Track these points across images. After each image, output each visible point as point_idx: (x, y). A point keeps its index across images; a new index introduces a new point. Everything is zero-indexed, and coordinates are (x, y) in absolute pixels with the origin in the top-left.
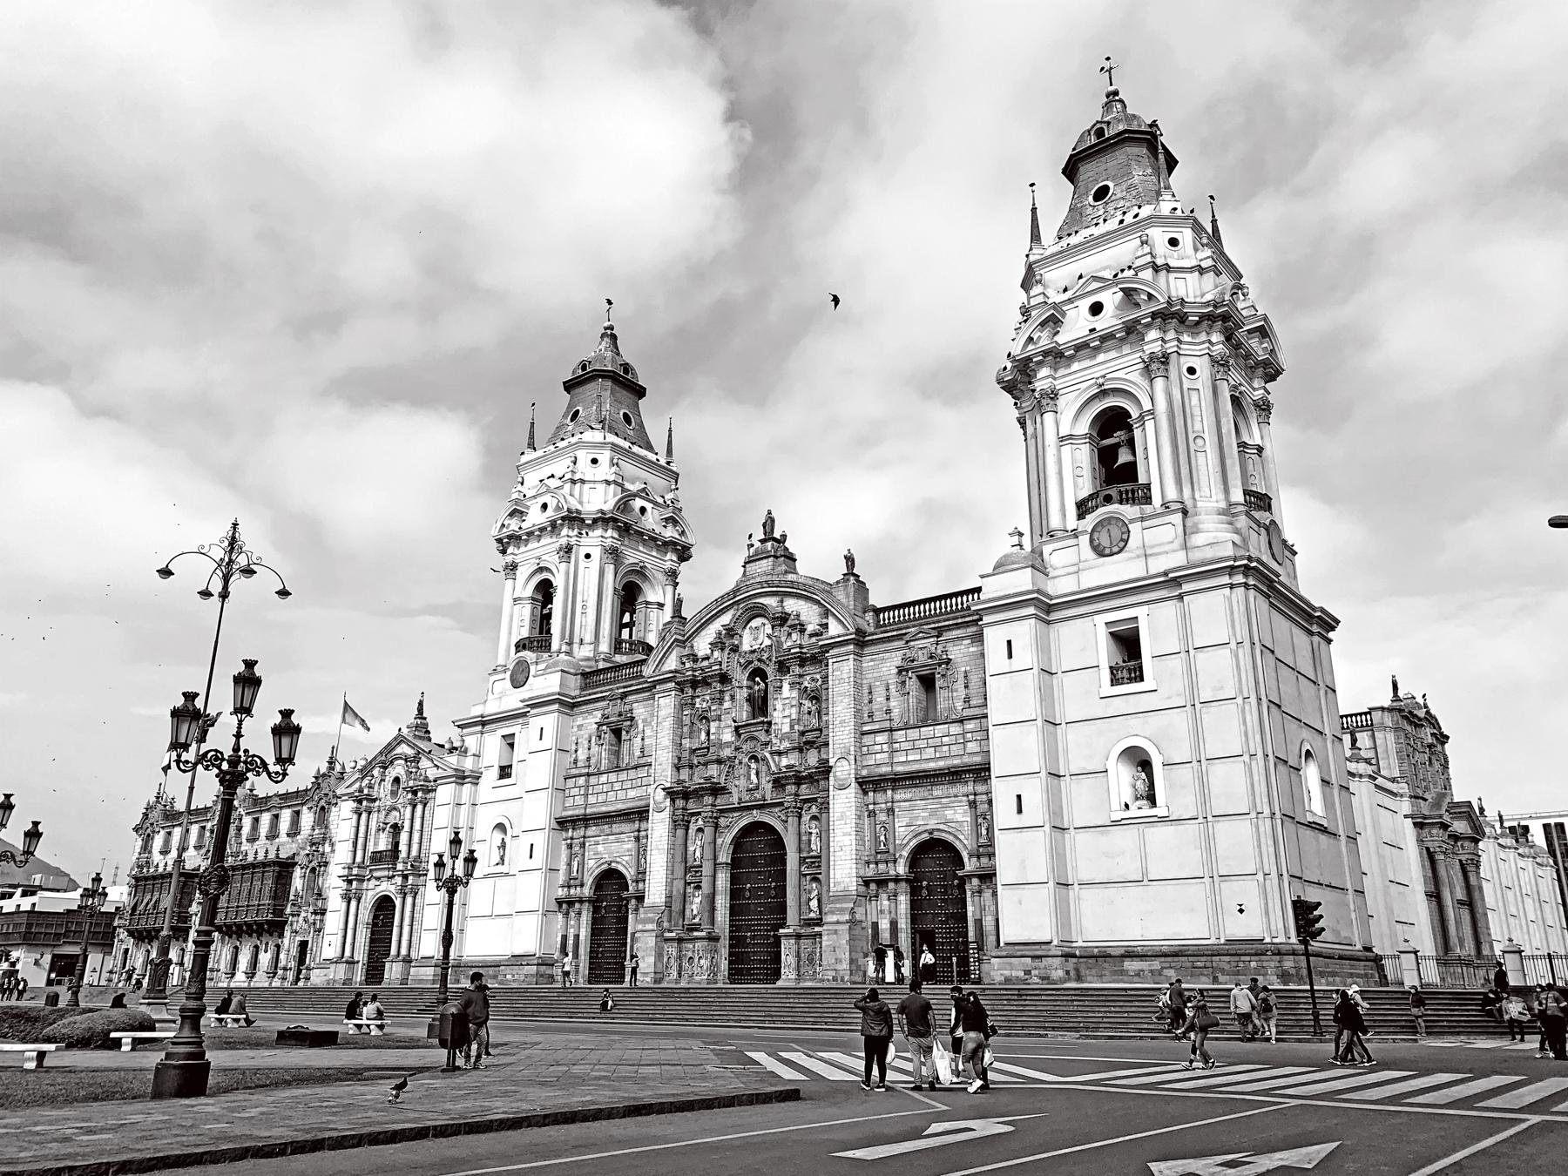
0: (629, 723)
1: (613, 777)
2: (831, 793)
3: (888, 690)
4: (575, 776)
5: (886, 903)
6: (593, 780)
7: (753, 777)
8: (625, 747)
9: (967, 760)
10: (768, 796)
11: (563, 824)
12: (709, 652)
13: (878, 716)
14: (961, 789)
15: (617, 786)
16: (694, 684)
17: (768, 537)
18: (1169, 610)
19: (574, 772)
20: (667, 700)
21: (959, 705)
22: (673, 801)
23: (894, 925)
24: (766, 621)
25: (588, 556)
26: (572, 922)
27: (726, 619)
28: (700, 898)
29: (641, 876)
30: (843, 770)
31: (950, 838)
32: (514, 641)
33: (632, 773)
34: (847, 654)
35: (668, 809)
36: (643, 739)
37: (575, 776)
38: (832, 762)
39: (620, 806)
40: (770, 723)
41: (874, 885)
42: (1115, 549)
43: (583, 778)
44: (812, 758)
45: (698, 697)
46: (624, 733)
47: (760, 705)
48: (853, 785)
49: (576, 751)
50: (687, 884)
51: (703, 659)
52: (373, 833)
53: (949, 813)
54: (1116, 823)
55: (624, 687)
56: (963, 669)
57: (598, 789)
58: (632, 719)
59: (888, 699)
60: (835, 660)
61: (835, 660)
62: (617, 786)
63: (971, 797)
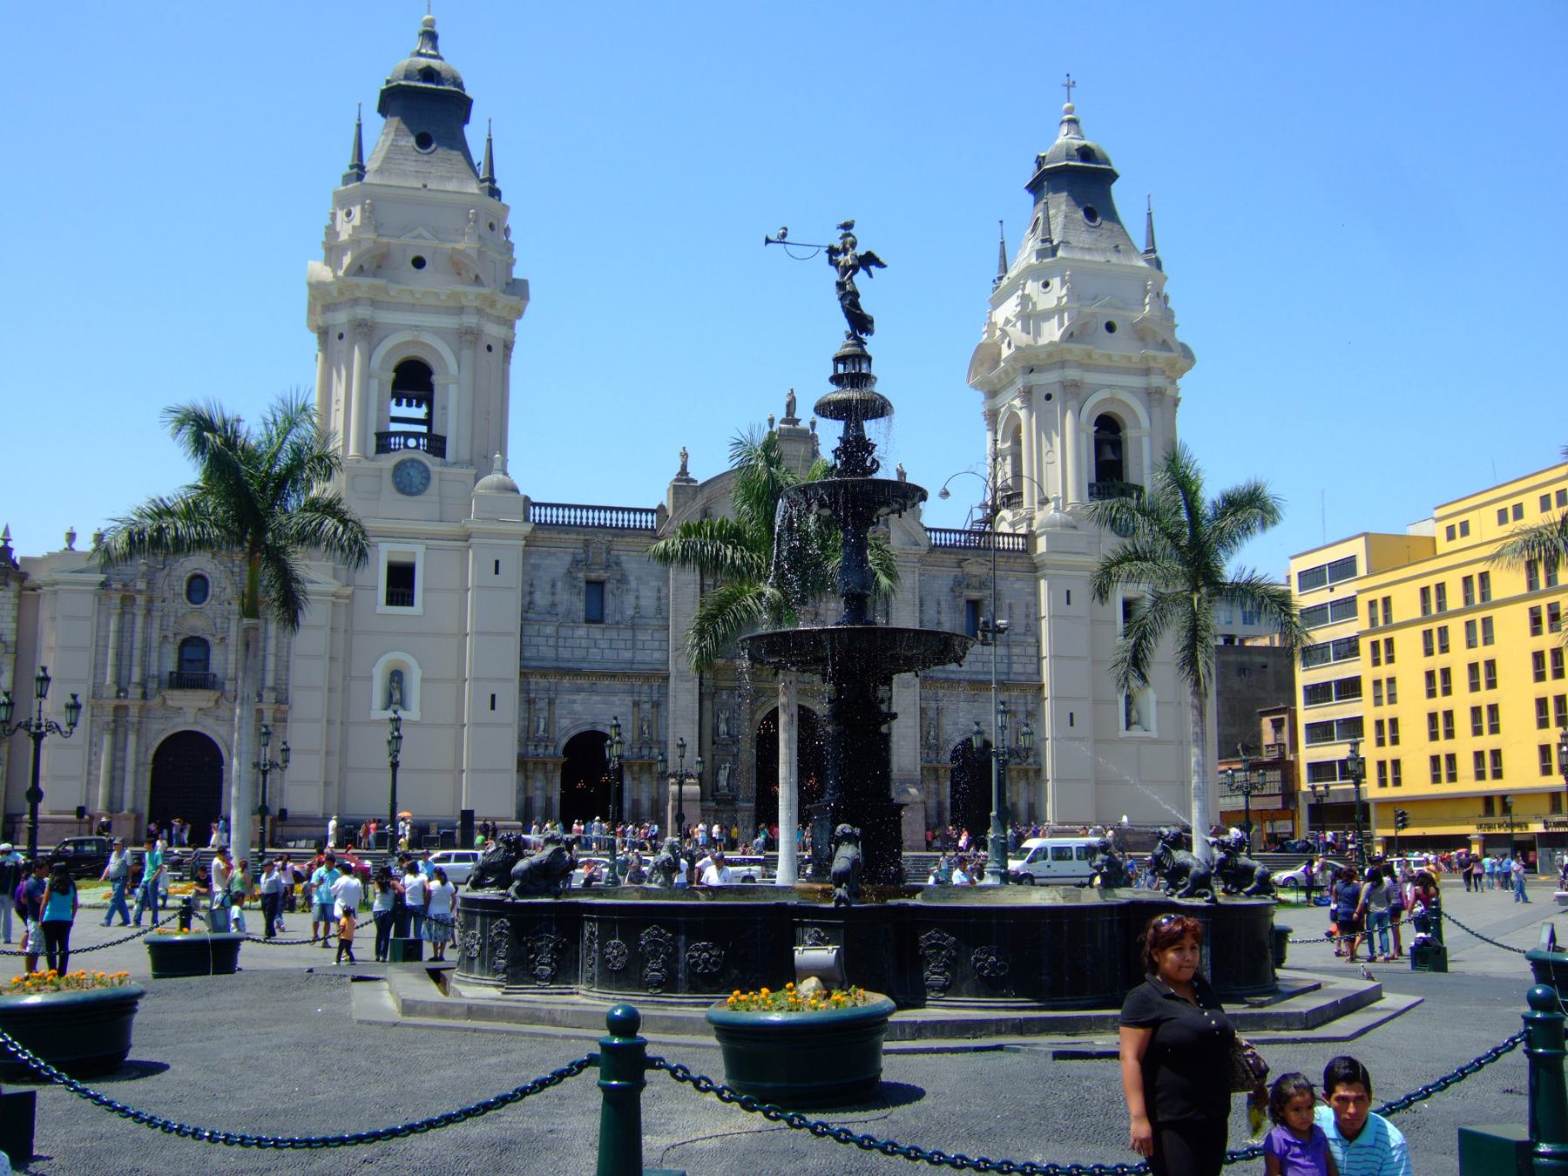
1: (596, 631)
3: (939, 604)
5: (933, 785)
6: (564, 632)
8: (610, 604)
9: (1012, 676)
11: (523, 675)
15: (603, 644)
17: (791, 418)
19: (531, 615)
23: (940, 804)
25: (489, 348)
26: (538, 784)
29: (651, 739)
32: (373, 429)
33: (628, 634)
34: (915, 567)
36: (637, 597)
41: (930, 771)
46: (608, 587)
49: (531, 593)
50: (713, 755)
52: (155, 643)
54: (1123, 740)
56: (1008, 601)
59: (939, 613)
62: (603, 644)
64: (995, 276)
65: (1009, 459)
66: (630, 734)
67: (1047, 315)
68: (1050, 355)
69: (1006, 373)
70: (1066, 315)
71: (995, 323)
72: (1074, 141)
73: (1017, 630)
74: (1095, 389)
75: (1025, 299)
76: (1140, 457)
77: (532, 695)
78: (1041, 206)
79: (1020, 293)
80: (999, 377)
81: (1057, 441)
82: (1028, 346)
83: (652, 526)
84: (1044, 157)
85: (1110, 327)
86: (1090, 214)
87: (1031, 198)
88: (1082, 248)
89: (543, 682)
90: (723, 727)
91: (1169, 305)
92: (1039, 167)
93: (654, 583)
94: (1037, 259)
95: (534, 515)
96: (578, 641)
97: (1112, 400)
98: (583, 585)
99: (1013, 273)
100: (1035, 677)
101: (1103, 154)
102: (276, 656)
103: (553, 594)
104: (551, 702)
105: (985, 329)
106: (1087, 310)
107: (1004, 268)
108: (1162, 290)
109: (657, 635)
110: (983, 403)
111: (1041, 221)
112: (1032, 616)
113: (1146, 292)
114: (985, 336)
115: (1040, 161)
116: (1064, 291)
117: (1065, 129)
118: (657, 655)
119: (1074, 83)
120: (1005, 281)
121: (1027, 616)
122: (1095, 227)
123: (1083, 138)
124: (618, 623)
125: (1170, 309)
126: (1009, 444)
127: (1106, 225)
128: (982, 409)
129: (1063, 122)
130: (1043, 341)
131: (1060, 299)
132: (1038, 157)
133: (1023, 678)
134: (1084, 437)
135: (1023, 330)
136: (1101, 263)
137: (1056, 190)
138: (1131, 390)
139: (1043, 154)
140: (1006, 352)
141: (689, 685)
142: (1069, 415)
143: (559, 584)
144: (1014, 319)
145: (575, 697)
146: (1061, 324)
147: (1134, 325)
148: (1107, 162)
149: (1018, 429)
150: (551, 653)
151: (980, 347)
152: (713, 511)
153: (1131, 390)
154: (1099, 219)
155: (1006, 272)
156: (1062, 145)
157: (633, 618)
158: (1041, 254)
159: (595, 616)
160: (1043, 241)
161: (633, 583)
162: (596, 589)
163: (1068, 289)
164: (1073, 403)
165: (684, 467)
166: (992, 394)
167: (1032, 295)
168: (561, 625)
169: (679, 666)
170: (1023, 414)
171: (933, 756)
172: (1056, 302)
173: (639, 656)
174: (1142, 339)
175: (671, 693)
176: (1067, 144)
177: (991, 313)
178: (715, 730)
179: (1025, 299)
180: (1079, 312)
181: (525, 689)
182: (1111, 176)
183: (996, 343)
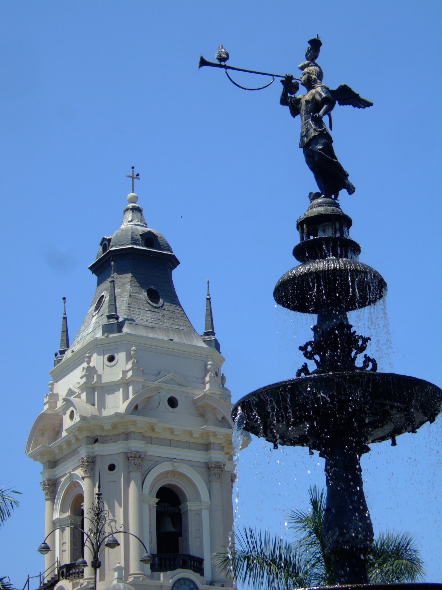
64: (58, 349)
65: (68, 531)
67: (112, 388)
68: (114, 426)
69: (68, 443)
70: (131, 389)
71: (57, 395)
72: (139, 228)
74: (158, 461)
75: (90, 372)
76: (200, 530)
78: (107, 284)
79: (85, 365)
80: (60, 448)
81: (120, 511)
82: (93, 417)
84: (109, 240)
85: (173, 402)
86: (153, 296)
87: (95, 278)
88: (146, 326)
91: (226, 386)
92: (105, 248)
94: (103, 334)
97: (174, 473)
99: (76, 346)
101: (165, 241)
105: (46, 400)
106: (151, 385)
107: (67, 343)
108: (219, 370)
110: (42, 473)
111: (107, 299)
113: (206, 371)
114: (46, 407)
115: (105, 243)
116: (130, 365)
117: (129, 216)
119: (138, 175)
120: (68, 354)
122: (158, 308)
123: (146, 225)
125: (226, 389)
126: (68, 514)
127: (167, 306)
128: (41, 479)
129: (127, 209)
130: (108, 412)
131: (125, 373)
132: (104, 239)
134: (146, 507)
135: (88, 401)
136: (163, 341)
137: (121, 271)
138: (193, 464)
139: (108, 238)
140: (67, 423)
142: (132, 485)
144: (77, 391)
146: (126, 397)
147: (194, 402)
148: (169, 249)
149: (80, 498)
151: (42, 417)
153: (193, 464)
154: (161, 301)
155: (68, 346)
156: (126, 230)
158: (107, 329)
160: (109, 317)
163: (133, 363)
164: (137, 475)
166: (53, 464)
167: (97, 368)
170: (85, 485)
172: (121, 375)
174: (202, 416)
176: (132, 229)
177: (53, 385)
179: (90, 372)
180: (144, 387)
182: (174, 262)
183: (57, 414)
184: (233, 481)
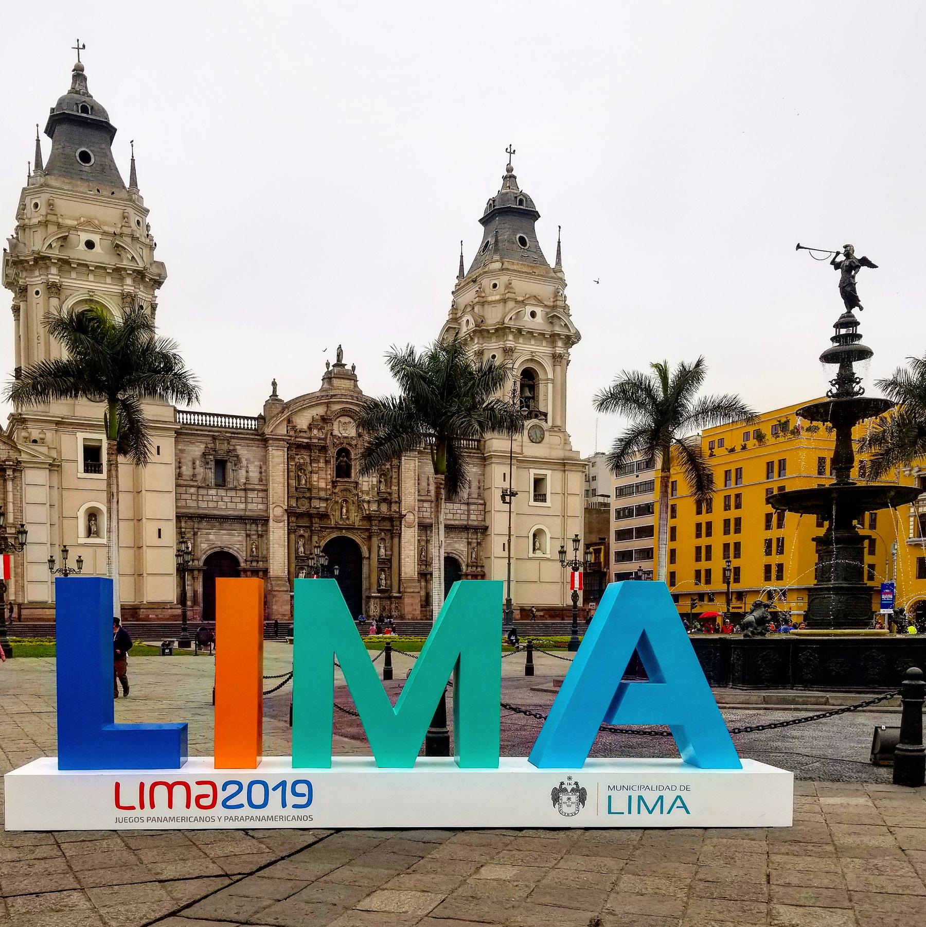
0: (235, 459)
1: (222, 492)
2: (403, 529)
3: (428, 479)
4: (186, 486)
6: (202, 492)
7: (344, 510)
8: (230, 474)
9: (470, 523)
10: (356, 524)
11: (179, 517)
12: (305, 427)
13: (423, 493)
14: (464, 535)
15: (227, 499)
16: (300, 446)
17: (339, 364)
18: (559, 475)
19: (182, 482)
20: (280, 453)
21: (466, 496)
22: (288, 517)
24: (351, 420)
27: (320, 411)
28: (304, 574)
30: (410, 518)
31: (457, 557)
33: (242, 494)
34: (415, 457)
35: (286, 521)
36: (247, 472)
37: (186, 486)
38: (404, 513)
39: (231, 513)
40: (357, 483)
42: (538, 441)
43: (195, 489)
44: (384, 508)
45: (297, 455)
47: (343, 471)
48: (417, 526)
49: (180, 468)
51: (300, 431)
53: (457, 546)
55: (232, 433)
57: (205, 498)
58: (237, 456)
59: (428, 485)
60: (406, 458)
61: (406, 458)
62: (227, 499)
63: (470, 540)
66: (245, 553)
73: (473, 496)
77: (183, 530)
83: (255, 428)
89: (190, 523)
90: (301, 549)
93: (257, 463)
95: (179, 419)
96: (211, 497)
98: (212, 464)
100: (483, 523)
102: (13, 503)
103: (194, 469)
104: (195, 534)
109: (260, 494)
112: (482, 488)
118: (260, 506)
121: (479, 488)
124: (236, 487)
133: (476, 523)
141: (281, 524)
143: (198, 462)
145: (210, 531)
150: (194, 504)
152: (293, 420)
157: (245, 484)
159: (222, 483)
161: (244, 463)
162: (221, 465)
165: (275, 391)
168: (199, 487)
169: (275, 513)
171: (424, 567)
173: (250, 507)
175: (271, 529)
178: (297, 550)
181: (179, 528)
184: (568, 365)
